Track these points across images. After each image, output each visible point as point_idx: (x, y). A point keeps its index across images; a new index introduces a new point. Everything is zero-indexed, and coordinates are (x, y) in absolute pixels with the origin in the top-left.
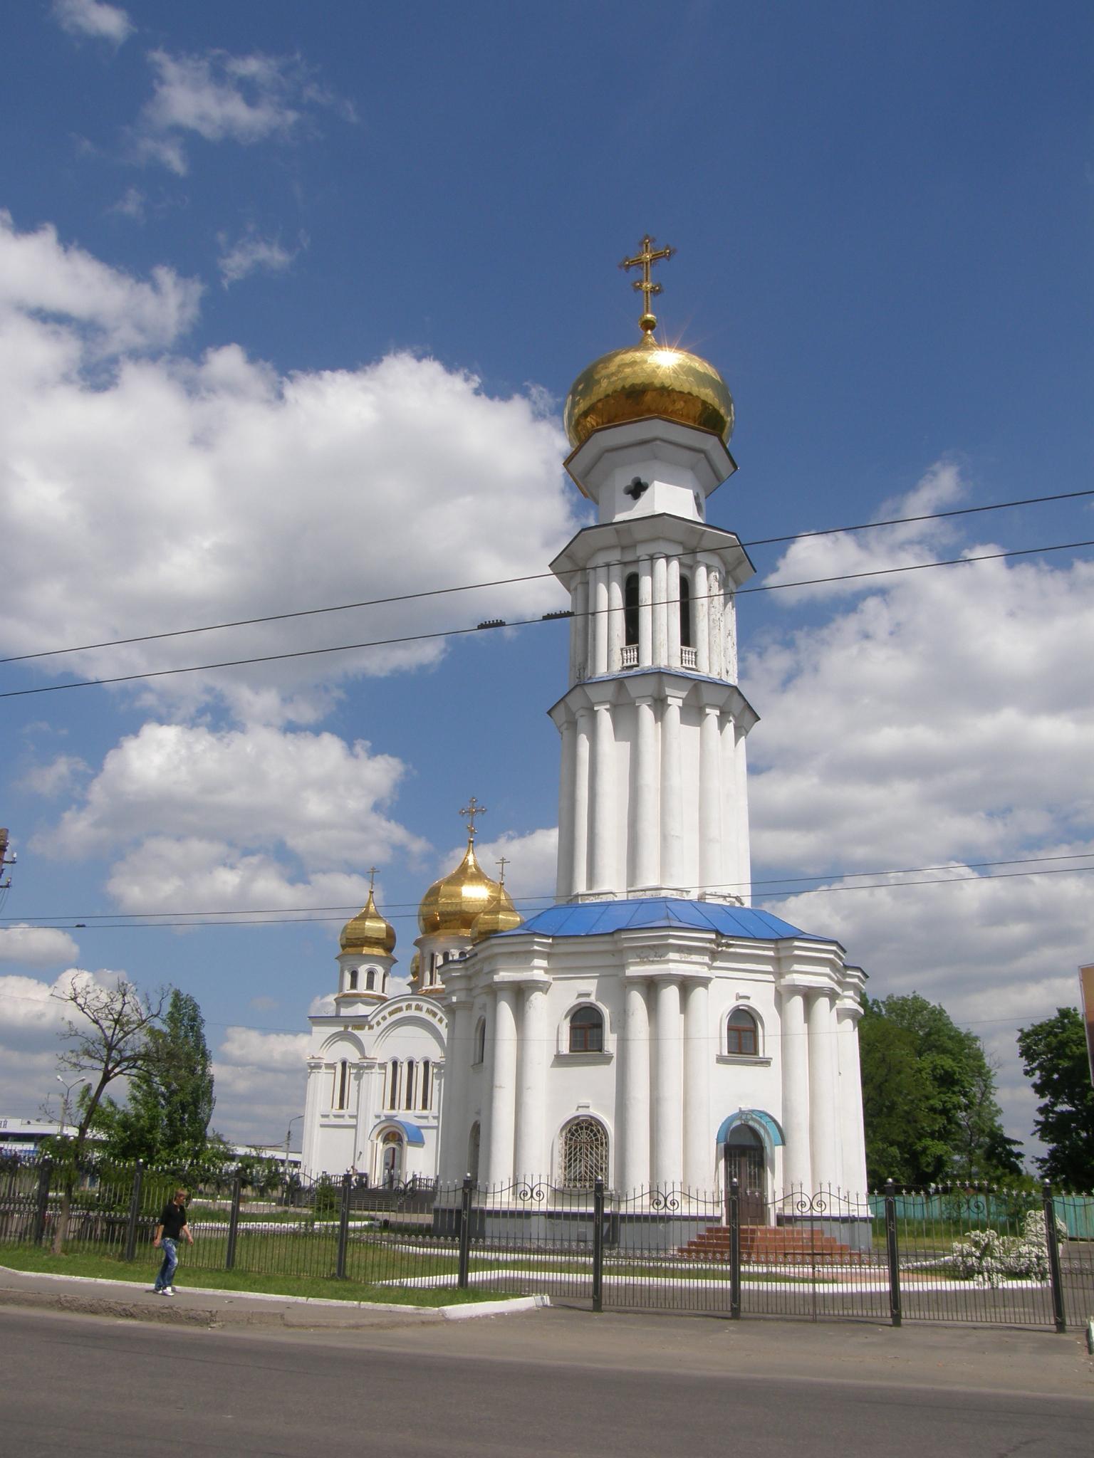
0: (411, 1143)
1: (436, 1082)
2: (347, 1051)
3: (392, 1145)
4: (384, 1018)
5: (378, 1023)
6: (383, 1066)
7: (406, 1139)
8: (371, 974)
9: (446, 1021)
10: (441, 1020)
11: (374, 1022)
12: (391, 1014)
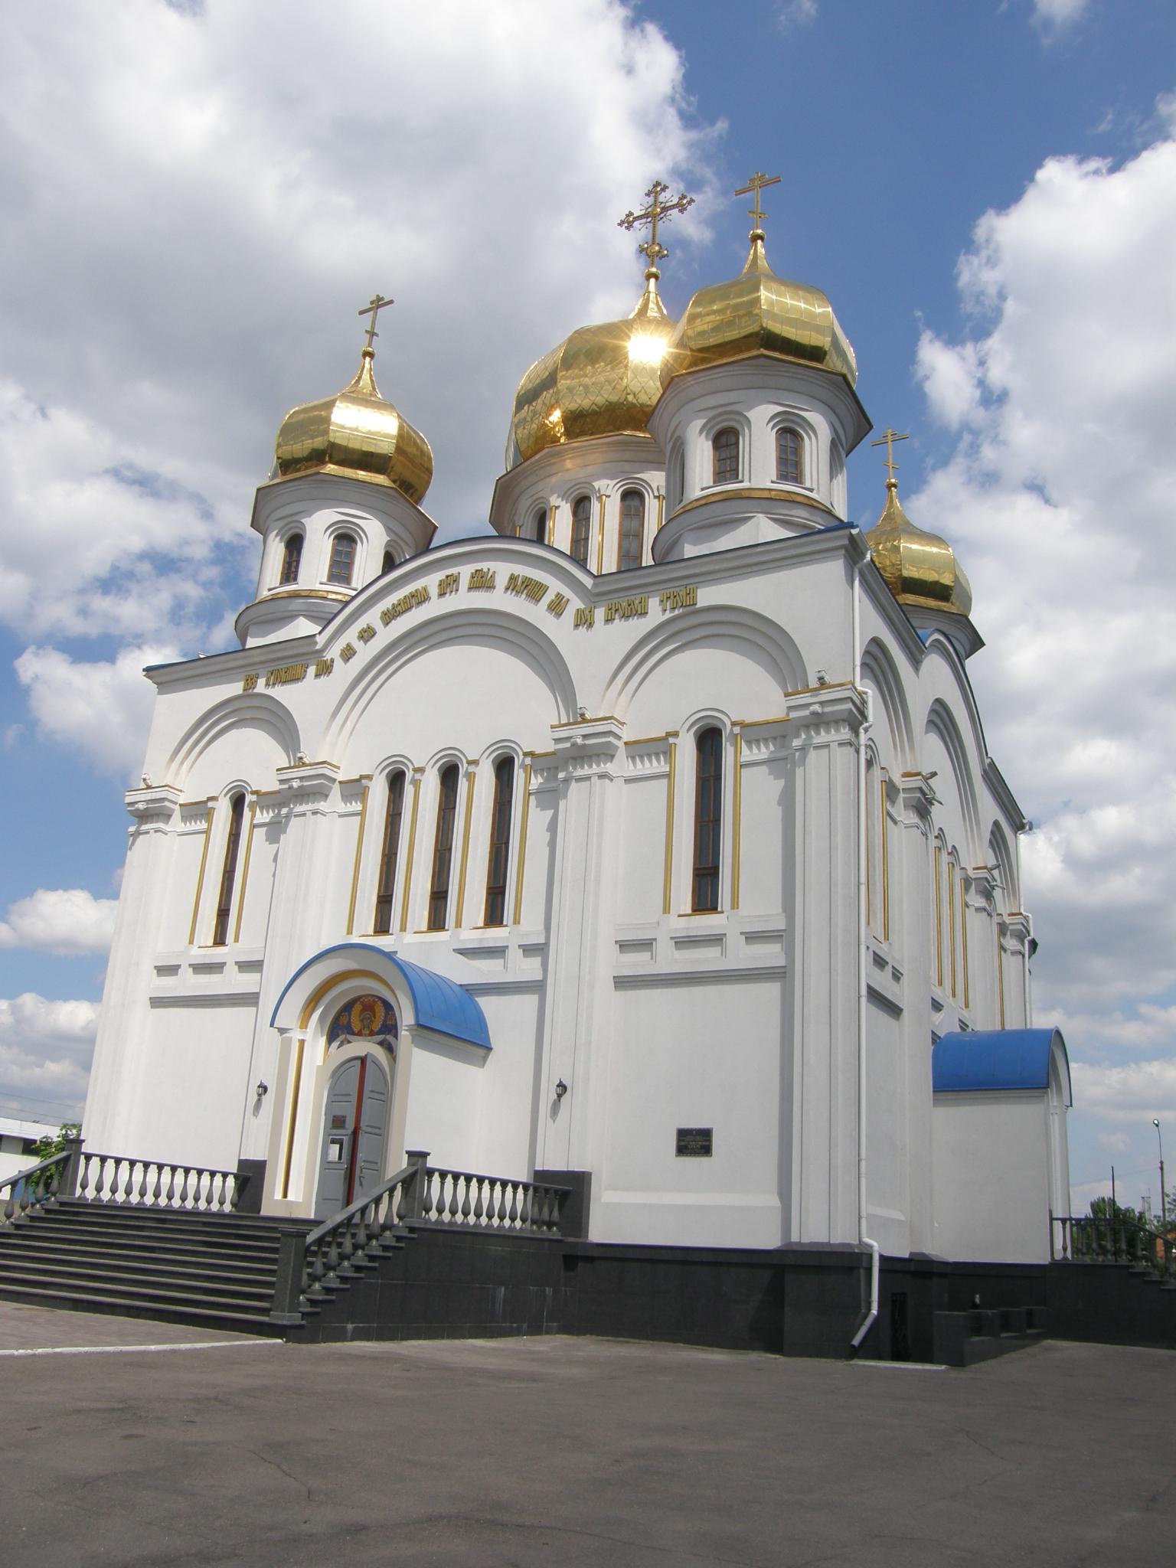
0: (429, 1032)
1: (539, 818)
2: (252, 758)
3: (361, 1047)
4: (367, 634)
5: (348, 653)
6: (356, 789)
7: (406, 1017)
8: (345, 540)
9: (575, 603)
10: (557, 607)
11: (334, 653)
12: (388, 617)
